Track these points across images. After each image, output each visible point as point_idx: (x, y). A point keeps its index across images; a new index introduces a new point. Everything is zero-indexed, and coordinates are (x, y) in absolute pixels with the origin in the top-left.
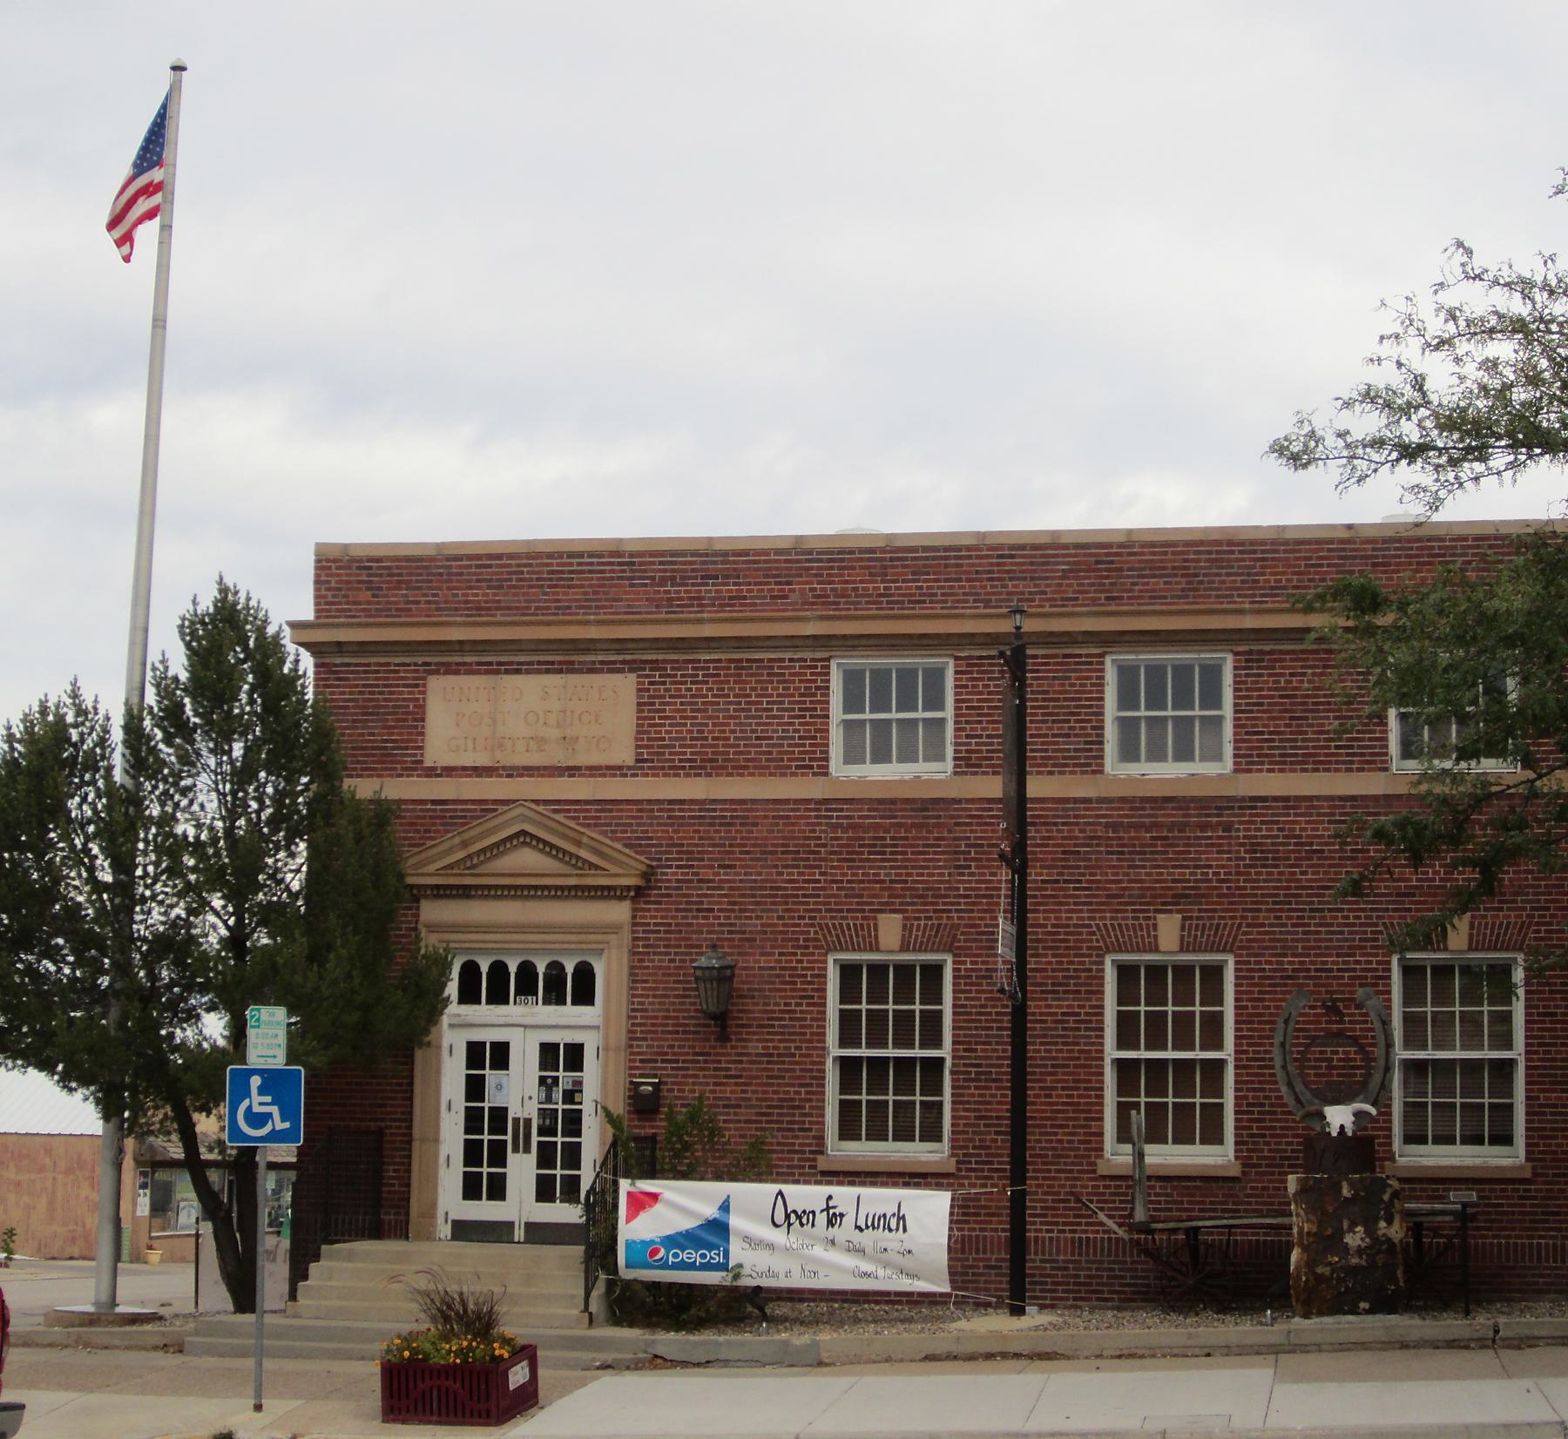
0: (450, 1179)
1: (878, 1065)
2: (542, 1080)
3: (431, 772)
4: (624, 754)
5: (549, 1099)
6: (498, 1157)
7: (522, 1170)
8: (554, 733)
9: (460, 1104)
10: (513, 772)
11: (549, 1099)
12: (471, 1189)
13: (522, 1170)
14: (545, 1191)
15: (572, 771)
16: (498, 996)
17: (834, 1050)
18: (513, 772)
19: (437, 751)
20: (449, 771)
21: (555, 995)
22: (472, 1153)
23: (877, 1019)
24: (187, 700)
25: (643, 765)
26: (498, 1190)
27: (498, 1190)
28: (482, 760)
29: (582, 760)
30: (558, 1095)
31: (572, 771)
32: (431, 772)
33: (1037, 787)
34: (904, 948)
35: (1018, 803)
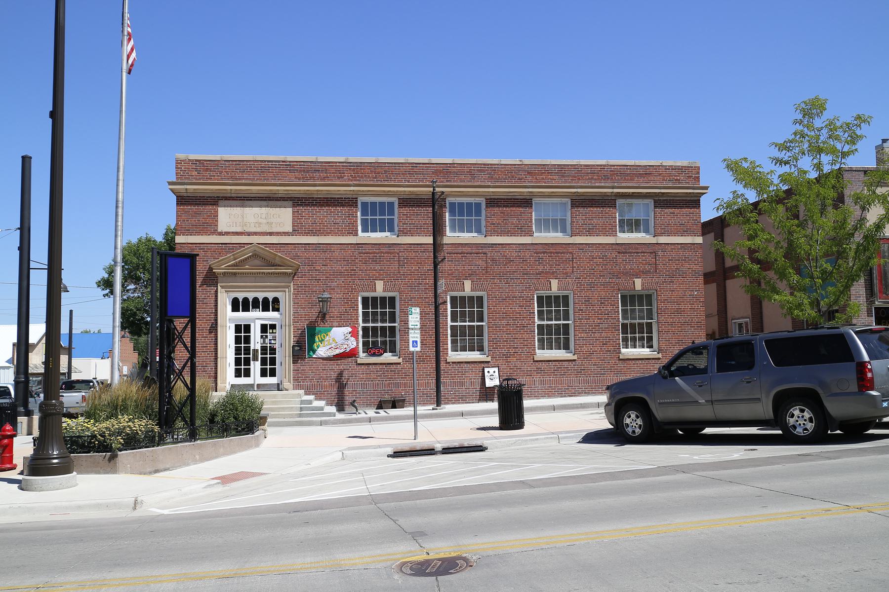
0: (231, 369)
1: (375, 329)
2: (262, 337)
3: (221, 234)
4: (289, 229)
5: (264, 342)
6: (247, 362)
7: (256, 367)
8: (265, 221)
9: (233, 345)
10: (249, 234)
11: (264, 342)
12: (238, 374)
13: (256, 367)
14: (263, 374)
15: (271, 234)
16: (246, 309)
17: (361, 324)
18: (249, 234)
19: (221, 228)
20: (227, 233)
21: (266, 309)
22: (238, 362)
23: (375, 314)
24: (866, 358)
25: (295, 232)
26: (247, 374)
27: (247, 374)
28: (239, 230)
29: (274, 230)
30: (267, 341)
31: (271, 234)
32: (221, 234)
33: (430, 240)
34: (384, 291)
35: (437, 246)
